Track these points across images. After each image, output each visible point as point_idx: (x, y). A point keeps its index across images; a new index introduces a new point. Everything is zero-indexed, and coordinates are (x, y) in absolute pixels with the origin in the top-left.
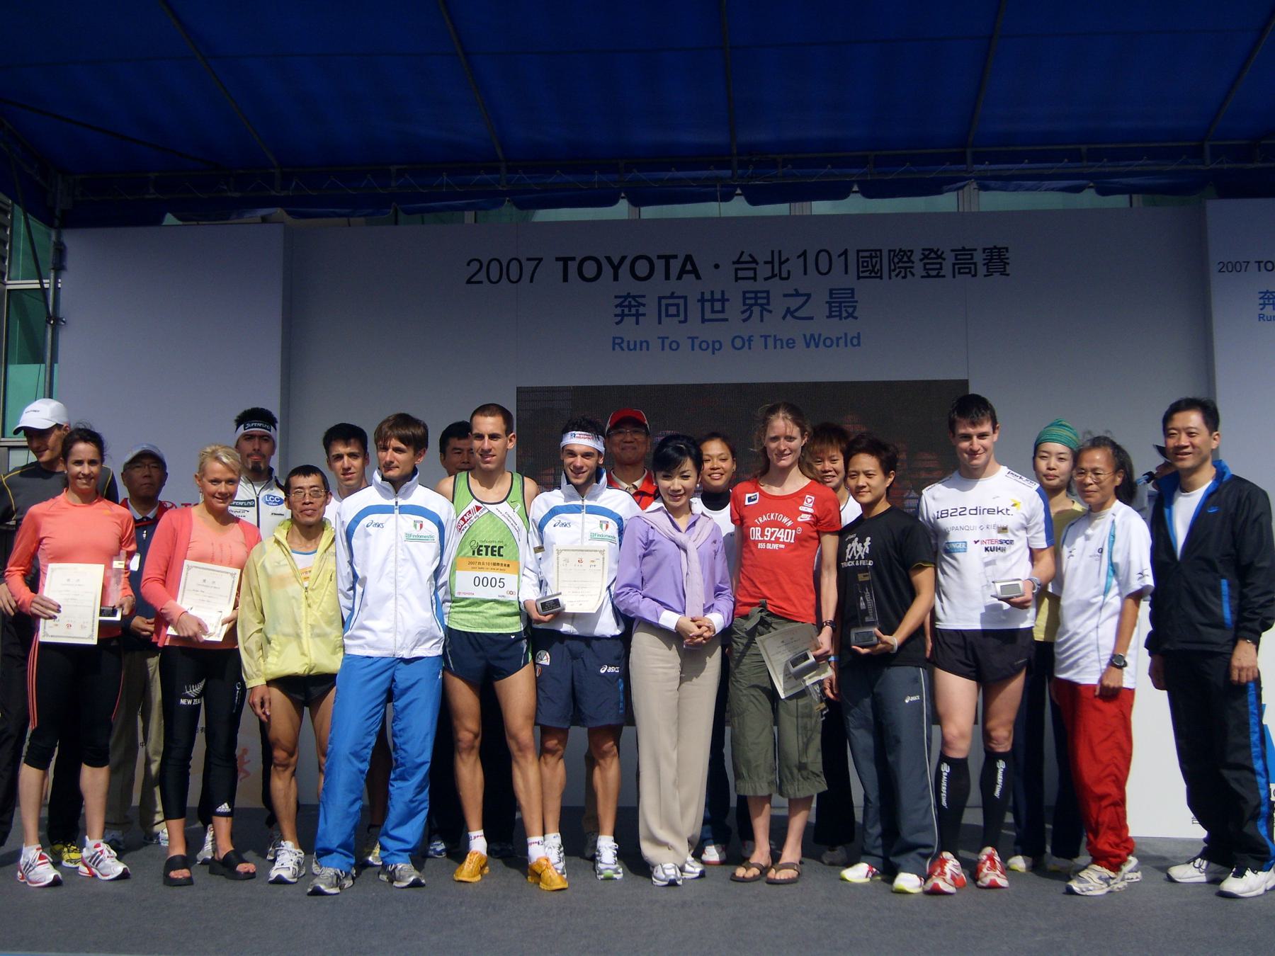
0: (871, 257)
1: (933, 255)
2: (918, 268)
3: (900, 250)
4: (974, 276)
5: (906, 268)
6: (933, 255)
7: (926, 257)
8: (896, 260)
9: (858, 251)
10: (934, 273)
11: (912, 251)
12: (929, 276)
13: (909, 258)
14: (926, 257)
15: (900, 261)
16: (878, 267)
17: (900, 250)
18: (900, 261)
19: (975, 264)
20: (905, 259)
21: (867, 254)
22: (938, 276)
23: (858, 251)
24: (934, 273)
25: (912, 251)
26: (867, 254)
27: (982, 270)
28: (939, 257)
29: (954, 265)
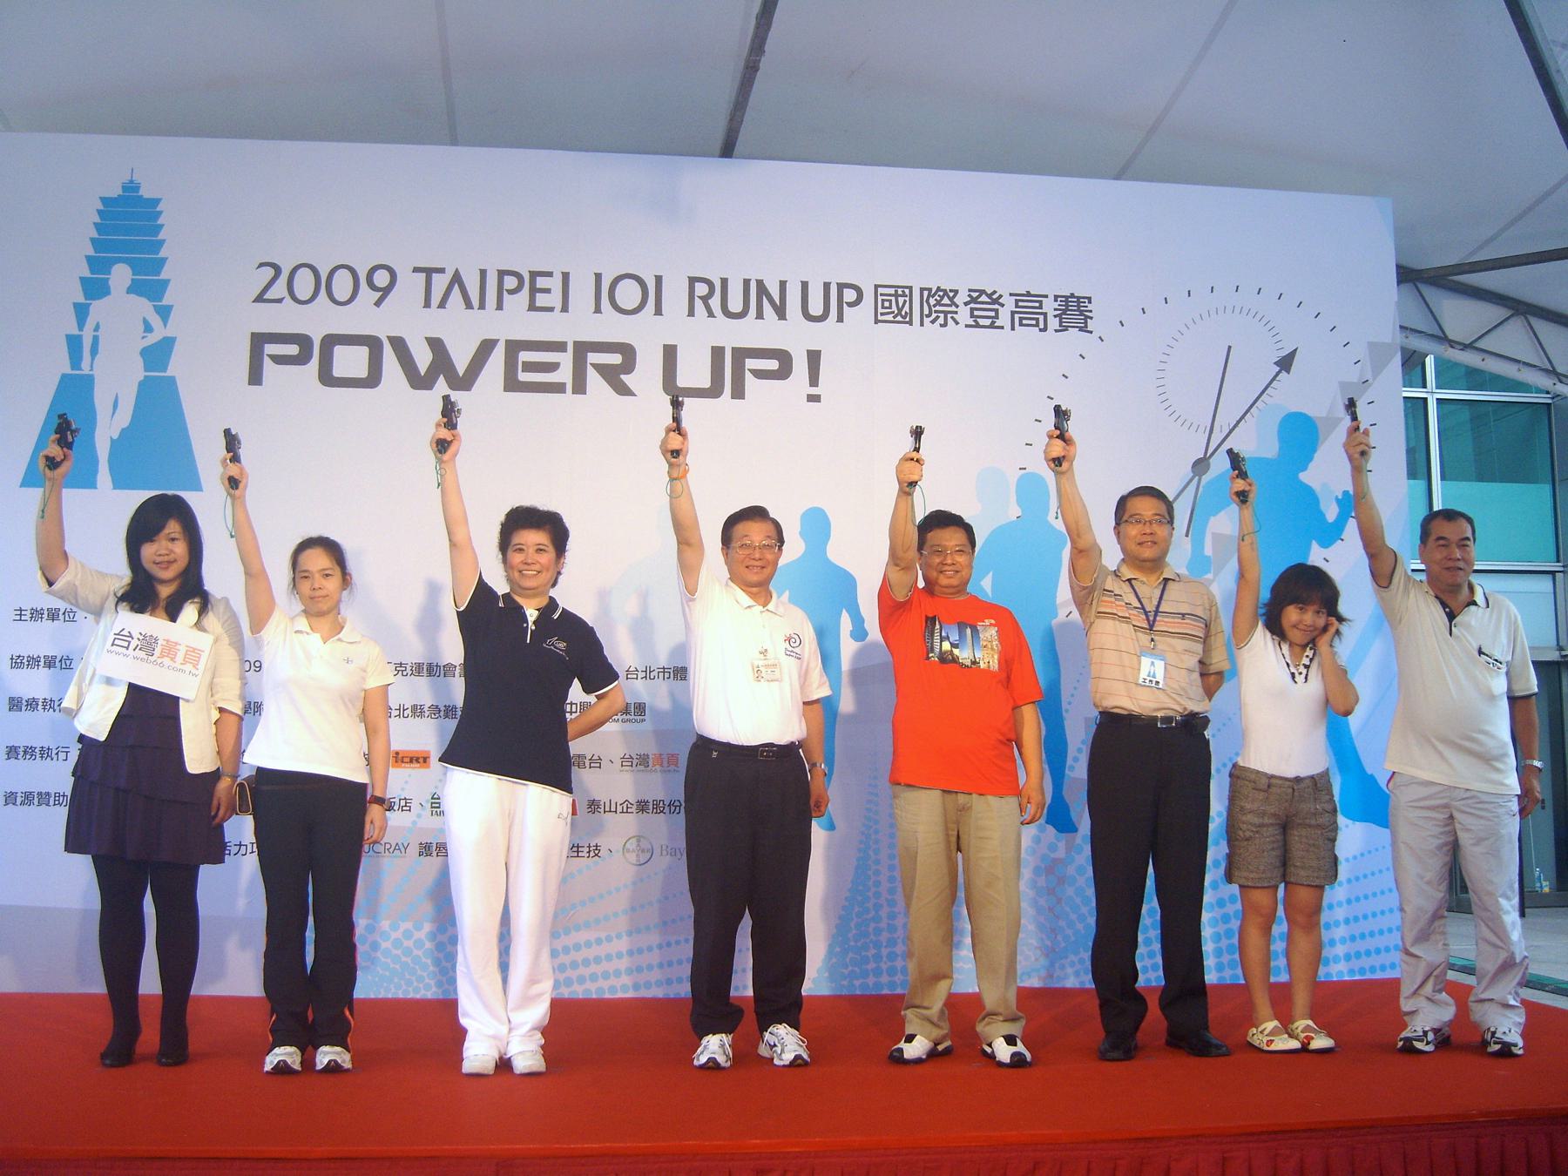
0: (896, 295)
1: (984, 298)
2: (964, 314)
3: (939, 289)
4: (1045, 329)
5: (946, 313)
6: (984, 298)
7: (974, 300)
8: (932, 301)
9: (876, 287)
10: (987, 322)
11: (956, 292)
12: (977, 326)
13: (951, 299)
14: (974, 300)
15: (938, 303)
16: (907, 308)
17: (939, 289)
18: (938, 303)
19: (1045, 314)
20: (946, 301)
21: (892, 291)
22: (992, 326)
23: (876, 287)
24: (987, 322)
25: (956, 292)
26: (892, 291)
27: (1053, 323)
28: (995, 302)
29: (1013, 313)
